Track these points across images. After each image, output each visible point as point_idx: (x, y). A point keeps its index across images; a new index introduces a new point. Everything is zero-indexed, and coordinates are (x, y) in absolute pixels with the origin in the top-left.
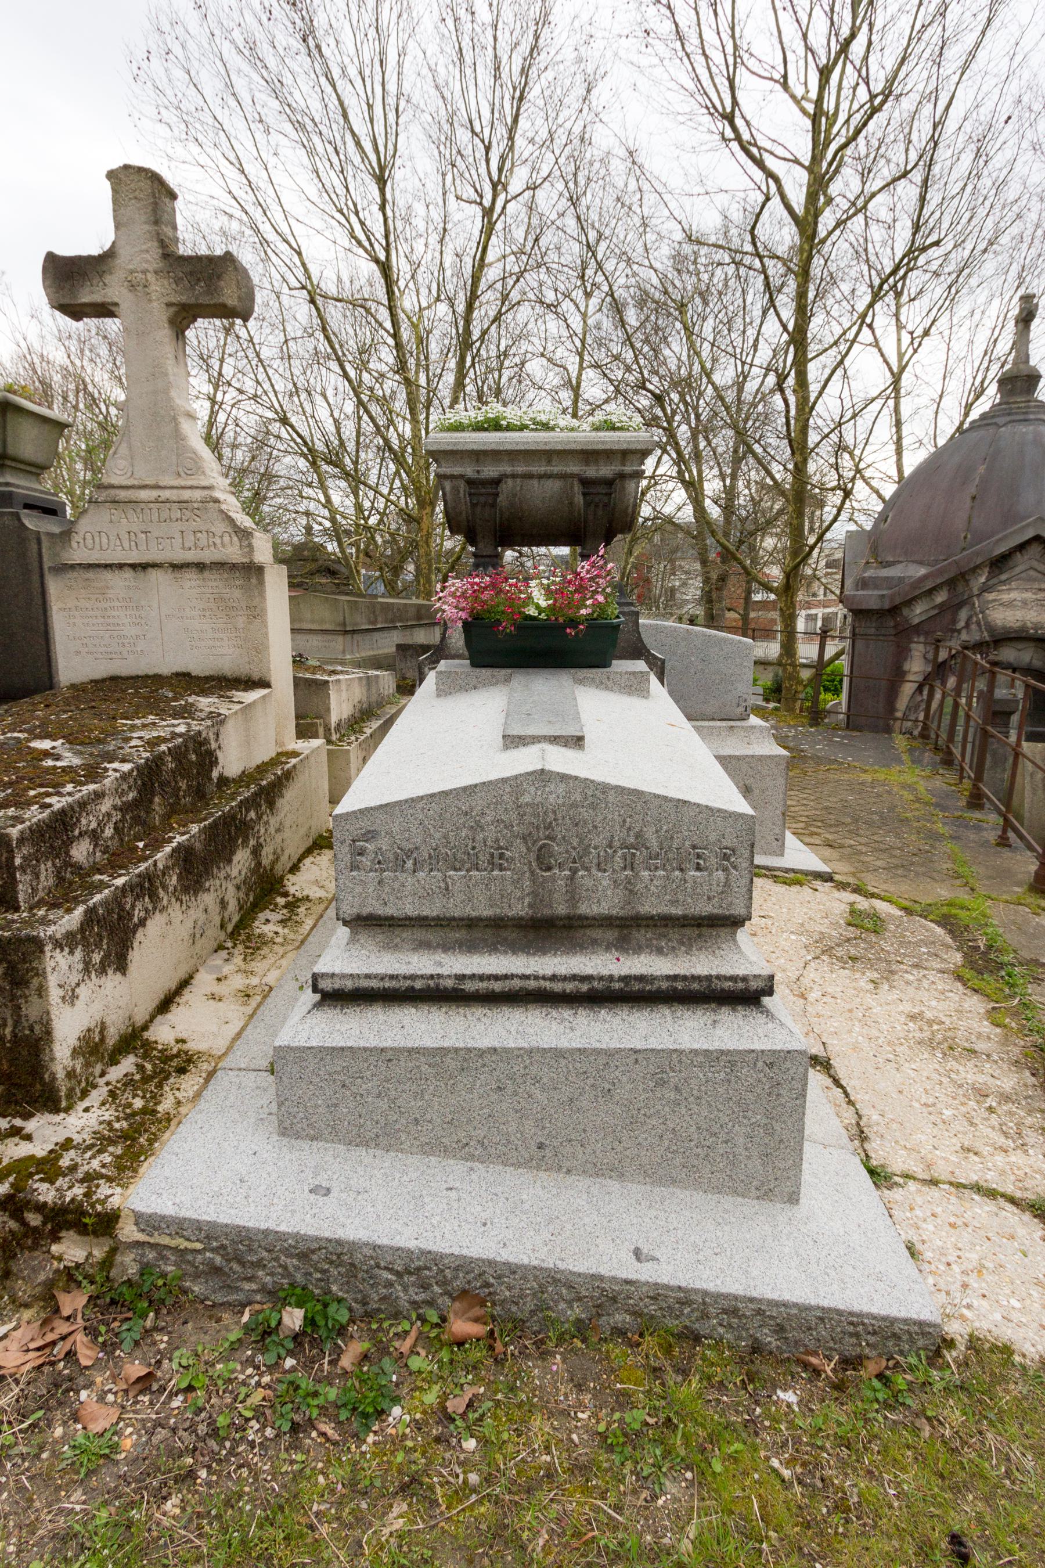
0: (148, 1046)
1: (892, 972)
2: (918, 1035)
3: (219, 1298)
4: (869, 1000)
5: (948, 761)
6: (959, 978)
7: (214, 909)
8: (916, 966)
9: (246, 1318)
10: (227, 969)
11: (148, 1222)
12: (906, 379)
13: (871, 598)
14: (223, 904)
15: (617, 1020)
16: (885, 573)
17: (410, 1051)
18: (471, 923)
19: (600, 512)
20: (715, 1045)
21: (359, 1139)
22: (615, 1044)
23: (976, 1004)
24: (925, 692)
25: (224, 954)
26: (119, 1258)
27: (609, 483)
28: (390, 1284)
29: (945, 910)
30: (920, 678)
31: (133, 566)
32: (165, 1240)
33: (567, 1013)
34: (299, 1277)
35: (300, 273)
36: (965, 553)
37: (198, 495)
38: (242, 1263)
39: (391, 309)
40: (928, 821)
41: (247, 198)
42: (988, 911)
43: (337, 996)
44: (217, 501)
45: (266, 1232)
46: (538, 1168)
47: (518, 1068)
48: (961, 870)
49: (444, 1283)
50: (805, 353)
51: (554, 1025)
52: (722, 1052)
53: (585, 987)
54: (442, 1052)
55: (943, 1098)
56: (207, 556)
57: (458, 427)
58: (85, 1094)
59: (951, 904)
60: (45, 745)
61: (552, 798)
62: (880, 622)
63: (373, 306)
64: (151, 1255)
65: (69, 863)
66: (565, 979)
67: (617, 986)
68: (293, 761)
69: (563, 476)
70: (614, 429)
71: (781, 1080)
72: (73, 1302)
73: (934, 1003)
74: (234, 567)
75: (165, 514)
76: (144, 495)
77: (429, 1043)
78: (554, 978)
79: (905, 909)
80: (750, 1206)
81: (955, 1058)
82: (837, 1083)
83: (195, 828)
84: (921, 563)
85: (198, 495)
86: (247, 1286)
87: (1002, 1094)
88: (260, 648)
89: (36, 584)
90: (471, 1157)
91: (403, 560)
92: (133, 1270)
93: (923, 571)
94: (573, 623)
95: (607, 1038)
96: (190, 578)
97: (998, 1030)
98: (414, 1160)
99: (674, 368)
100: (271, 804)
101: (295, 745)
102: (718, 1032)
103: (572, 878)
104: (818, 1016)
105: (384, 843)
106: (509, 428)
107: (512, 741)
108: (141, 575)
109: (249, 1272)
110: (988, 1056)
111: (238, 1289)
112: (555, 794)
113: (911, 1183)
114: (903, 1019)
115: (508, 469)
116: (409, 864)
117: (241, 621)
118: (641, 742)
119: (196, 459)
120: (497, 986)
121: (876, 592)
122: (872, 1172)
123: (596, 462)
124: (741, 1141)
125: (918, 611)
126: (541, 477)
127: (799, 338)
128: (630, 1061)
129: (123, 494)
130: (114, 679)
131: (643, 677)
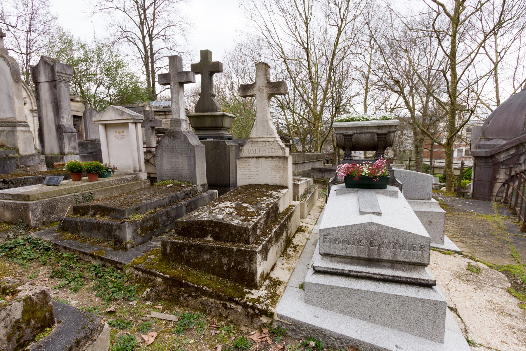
0: (271, 279)
1: (482, 286)
2: (490, 307)
3: (294, 336)
4: (473, 294)
5: (515, 213)
6: (508, 292)
7: (280, 246)
8: (492, 286)
9: (301, 342)
10: (283, 262)
11: (280, 316)
12: (499, 65)
13: (482, 152)
14: (281, 245)
15: (391, 287)
16: (488, 143)
17: (337, 287)
18: (352, 258)
19: (382, 142)
20: (419, 297)
21: (323, 307)
22: (390, 293)
23: (514, 301)
24: (506, 186)
25: (282, 258)
26: (273, 323)
27: (386, 134)
28: (333, 341)
29: (506, 268)
30: (504, 181)
31: (256, 157)
32: (283, 321)
33: (377, 283)
34: (312, 335)
35: (280, 52)
36: (523, 136)
37: (272, 139)
38: (299, 329)
39: (308, 61)
40: (503, 236)
41: (267, 33)
42: (524, 271)
43: (318, 272)
44: (277, 141)
45: (306, 323)
46: (369, 321)
47: (364, 295)
48: (514, 255)
49: (347, 343)
50: (455, 62)
51: (374, 286)
52: (421, 299)
53: (382, 277)
54: (345, 288)
55: (496, 326)
56: (274, 155)
57: (341, 121)
58: (261, 287)
59: (508, 267)
60: (245, 205)
61: (374, 229)
62: (487, 160)
63: (302, 60)
64: (280, 324)
65: (257, 235)
66: (377, 274)
67: (391, 278)
68: (294, 208)
69: (371, 133)
70: (387, 119)
71: (438, 309)
72: (265, 330)
73: (497, 298)
74: (280, 157)
75: (264, 144)
76: (259, 140)
77: (342, 286)
78: (374, 274)
79: (490, 267)
80: (429, 341)
81: (502, 315)
82: (459, 316)
83: (277, 226)
84: (504, 139)
85: (272, 139)
86: (300, 335)
87: (519, 329)
88: (286, 178)
89: (228, 158)
90: (351, 316)
91: (307, 134)
92: (276, 326)
93: (504, 142)
94: (375, 177)
95: (388, 291)
96: (270, 160)
97: (522, 310)
98: (337, 314)
99: (403, 67)
100: (290, 220)
101: (293, 203)
102: (420, 293)
103: (379, 249)
104: (454, 296)
105: (331, 237)
106: (355, 121)
107: (362, 213)
108: (258, 159)
109: (301, 332)
110: (516, 317)
111: (298, 335)
112: (375, 228)
113: (482, 347)
114: (484, 301)
115: (355, 131)
116: (337, 242)
117: (281, 171)
118: (396, 212)
119: (272, 130)
120: (359, 274)
121: (484, 150)
122: (468, 341)
123: (382, 129)
124: (426, 323)
125: (502, 157)
126: (365, 133)
127: (452, 56)
128: (395, 297)
129: (254, 140)
130: (250, 185)
131: (396, 192)
